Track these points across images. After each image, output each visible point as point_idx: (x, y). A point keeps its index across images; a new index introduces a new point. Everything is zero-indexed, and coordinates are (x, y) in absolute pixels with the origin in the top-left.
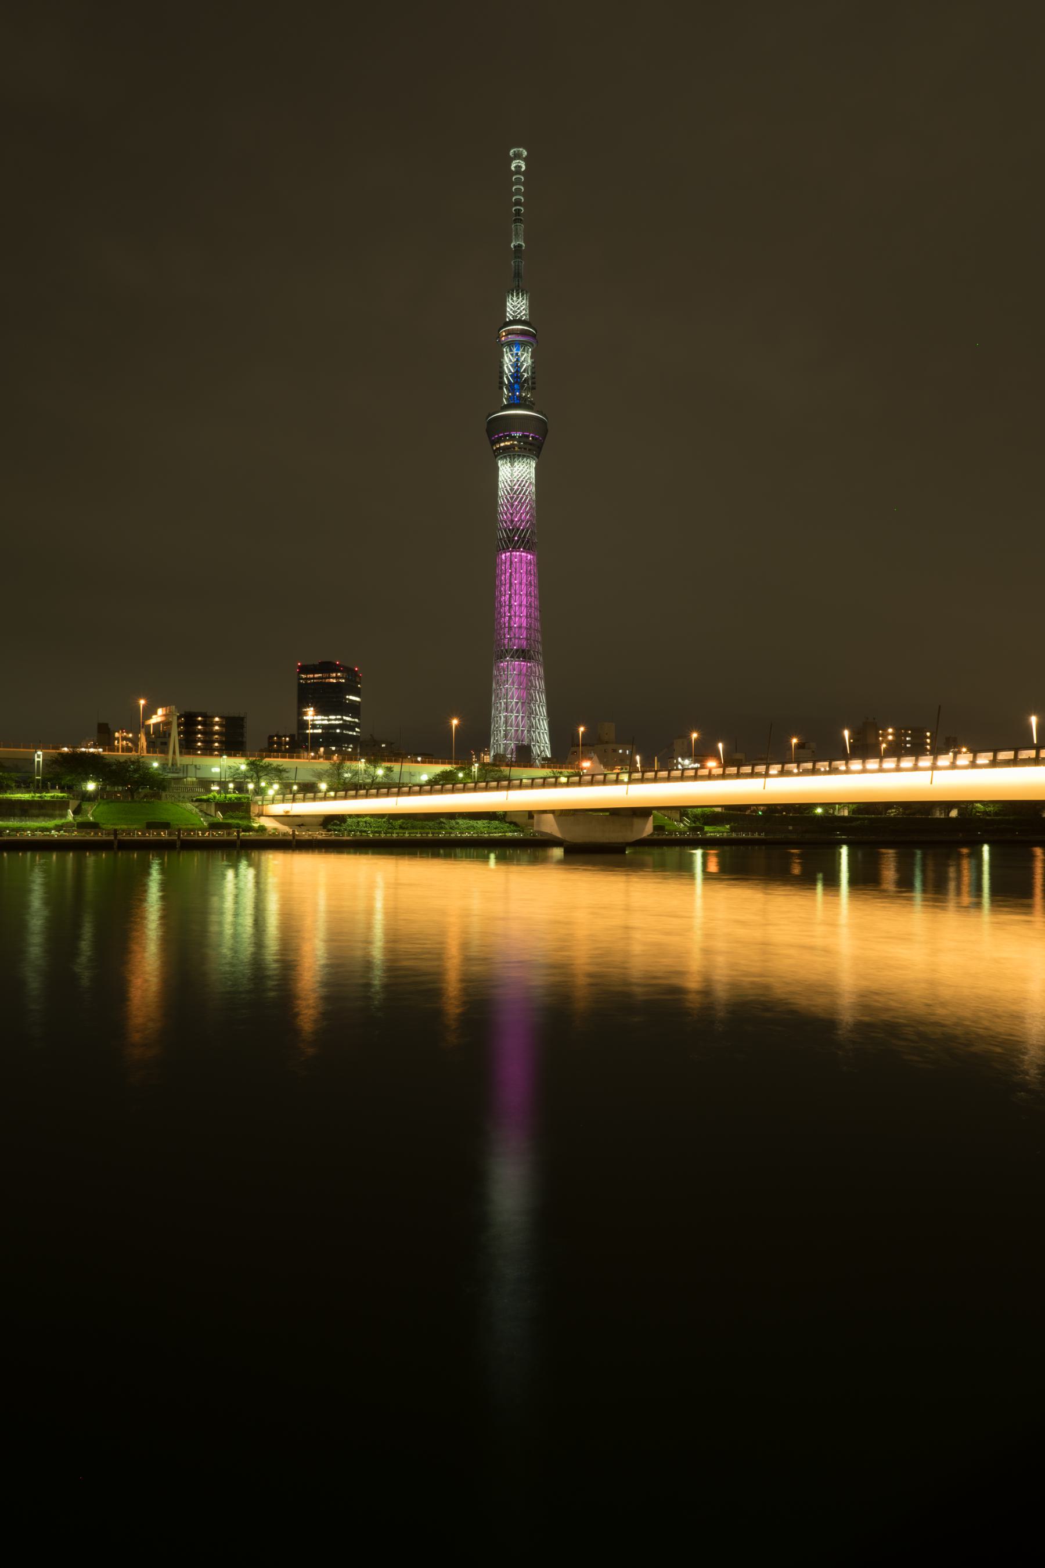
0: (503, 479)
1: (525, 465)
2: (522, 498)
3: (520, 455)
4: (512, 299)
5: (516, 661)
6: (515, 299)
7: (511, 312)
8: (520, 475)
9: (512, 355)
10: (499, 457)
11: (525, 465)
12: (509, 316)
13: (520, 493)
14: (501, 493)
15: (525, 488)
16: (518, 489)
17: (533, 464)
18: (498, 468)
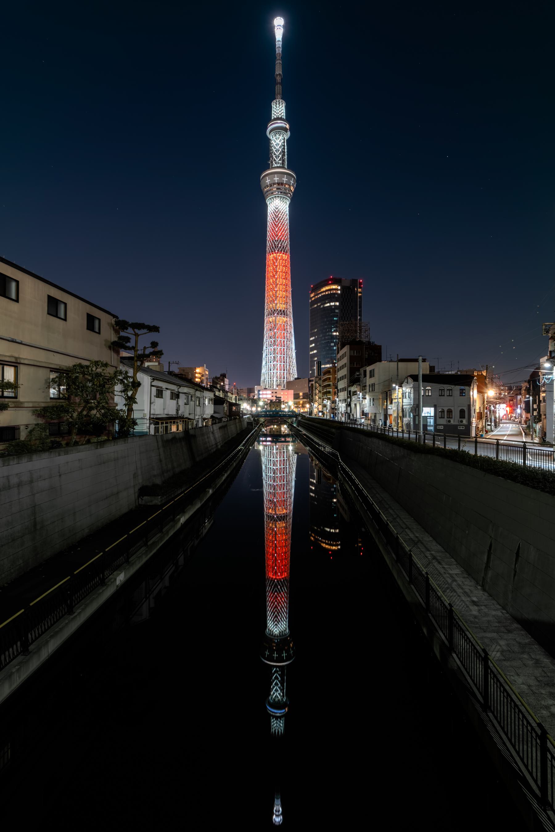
0: (272, 211)
1: (284, 203)
2: (283, 222)
3: (281, 197)
4: (276, 106)
5: (280, 317)
6: (278, 106)
7: (275, 113)
8: (281, 209)
9: (276, 138)
10: (268, 198)
11: (284, 203)
12: (273, 116)
13: (281, 219)
14: (269, 219)
15: (284, 216)
16: (280, 217)
17: (288, 203)
18: (266, 206)
